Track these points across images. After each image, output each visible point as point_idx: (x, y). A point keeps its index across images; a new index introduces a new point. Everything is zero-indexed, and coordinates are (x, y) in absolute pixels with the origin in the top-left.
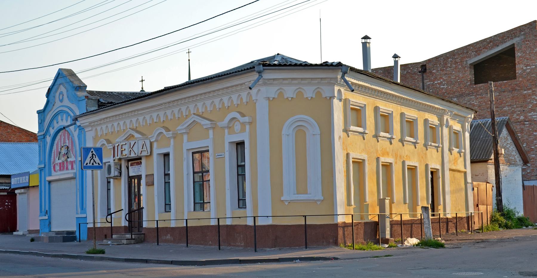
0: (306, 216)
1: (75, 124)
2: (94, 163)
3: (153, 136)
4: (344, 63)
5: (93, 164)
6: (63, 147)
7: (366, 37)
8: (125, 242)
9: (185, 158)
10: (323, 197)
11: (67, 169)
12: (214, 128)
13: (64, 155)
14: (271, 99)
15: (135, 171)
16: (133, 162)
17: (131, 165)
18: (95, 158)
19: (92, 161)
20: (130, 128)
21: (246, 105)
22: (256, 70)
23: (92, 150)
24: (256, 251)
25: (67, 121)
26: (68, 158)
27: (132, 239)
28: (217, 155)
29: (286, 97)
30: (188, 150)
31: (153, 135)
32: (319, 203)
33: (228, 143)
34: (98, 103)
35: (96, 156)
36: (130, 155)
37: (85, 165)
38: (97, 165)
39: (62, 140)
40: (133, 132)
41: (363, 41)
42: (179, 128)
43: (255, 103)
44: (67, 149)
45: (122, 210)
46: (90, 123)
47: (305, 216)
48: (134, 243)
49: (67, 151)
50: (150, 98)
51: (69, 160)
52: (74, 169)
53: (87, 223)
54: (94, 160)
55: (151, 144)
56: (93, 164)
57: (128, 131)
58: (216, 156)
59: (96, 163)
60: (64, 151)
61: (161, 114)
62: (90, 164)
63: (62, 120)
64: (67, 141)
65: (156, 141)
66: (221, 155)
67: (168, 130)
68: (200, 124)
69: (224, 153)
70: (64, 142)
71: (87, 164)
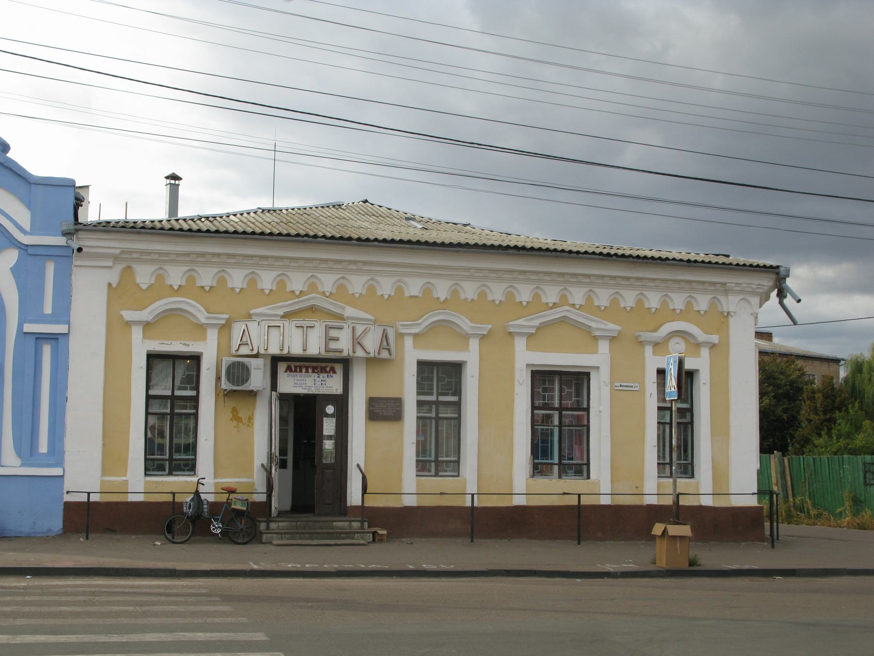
3: (419, 324)
7: (174, 177)
28: (618, 384)
41: (168, 181)
42: (520, 322)
50: (457, 252)
66: (631, 387)
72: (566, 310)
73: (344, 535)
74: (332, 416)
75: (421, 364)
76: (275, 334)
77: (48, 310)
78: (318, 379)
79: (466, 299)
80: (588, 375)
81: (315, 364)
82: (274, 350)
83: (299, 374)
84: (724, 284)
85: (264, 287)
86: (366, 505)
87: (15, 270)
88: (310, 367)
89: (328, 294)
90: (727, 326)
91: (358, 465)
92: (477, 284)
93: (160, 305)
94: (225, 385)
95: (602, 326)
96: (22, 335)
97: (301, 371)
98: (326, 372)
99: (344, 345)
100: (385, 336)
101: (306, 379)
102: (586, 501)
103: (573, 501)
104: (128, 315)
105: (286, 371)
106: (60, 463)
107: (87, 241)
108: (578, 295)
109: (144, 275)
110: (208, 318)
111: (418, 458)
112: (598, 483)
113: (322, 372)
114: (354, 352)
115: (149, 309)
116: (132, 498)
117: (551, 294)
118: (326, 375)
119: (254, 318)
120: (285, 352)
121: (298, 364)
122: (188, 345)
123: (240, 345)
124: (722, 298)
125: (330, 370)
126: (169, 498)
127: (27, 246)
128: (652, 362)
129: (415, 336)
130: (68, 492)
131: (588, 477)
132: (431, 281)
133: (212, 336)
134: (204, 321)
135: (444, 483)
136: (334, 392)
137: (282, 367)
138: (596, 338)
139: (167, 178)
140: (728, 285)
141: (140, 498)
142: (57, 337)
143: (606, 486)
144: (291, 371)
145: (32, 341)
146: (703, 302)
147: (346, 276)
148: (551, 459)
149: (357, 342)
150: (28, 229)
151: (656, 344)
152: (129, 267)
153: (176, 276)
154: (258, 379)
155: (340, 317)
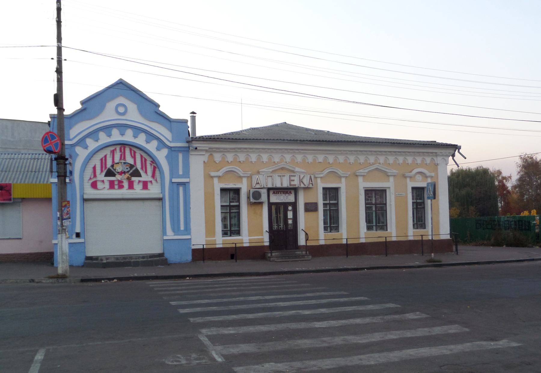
3: (323, 173)
28: (397, 194)
41: (191, 115)
42: (361, 171)
50: (338, 144)
66: (402, 194)
72: (378, 166)
74: (290, 210)
75: (324, 189)
76: (270, 179)
77: (181, 173)
78: (285, 196)
79: (340, 163)
80: (385, 190)
81: (284, 191)
82: (270, 186)
83: (278, 194)
84: (436, 153)
85: (252, 161)
86: (307, 245)
87: (167, 157)
88: (282, 192)
89: (288, 162)
90: (437, 169)
91: (302, 230)
92: (344, 156)
93: (224, 169)
94: (252, 200)
95: (391, 171)
96: (172, 183)
97: (278, 193)
98: (288, 193)
99: (296, 183)
100: (311, 178)
101: (280, 196)
102: (388, 240)
103: (383, 240)
104: (213, 174)
105: (273, 194)
106: (189, 234)
107: (195, 144)
108: (382, 159)
109: (218, 157)
110: (244, 174)
111: (324, 226)
112: (391, 233)
113: (286, 194)
114: (300, 185)
115: (221, 171)
116: (218, 246)
117: (372, 159)
118: (288, 195)
119: (261, 173)
120: (274, 186)
121: (277, 190)
122: (236, 185)
123: (256, 184)
124: (435, 158)
125: (289, 193)
126: (234, 246)
127: (171, 147)
128: (411, 184)
129: (321, 177)
130: (193, 245)
131: (387, 230)
132: (327, 156)
133: (245, 180)
134: (242, 175)
135: (333, 234)
136: (291, 201)
137: (271, 192)
138: (388, 176)
139: (191, 113)
140: (438, 153)
141: (221, 246)
142: (185, 183)
143: (394, 234)
144: (275, 194)
145: (175, 185)
146: (428, 160)
147: (295, 155)
148: (372, 224)
149: (301, 181)
150: (171, 140)
151: (411, 177)
152: (211, 154)
153: (230, 157)
154: (264, 198)
155: (293, 172)
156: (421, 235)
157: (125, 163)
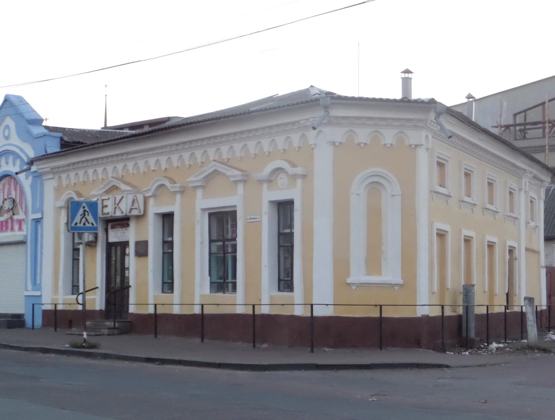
0: (382, 306)
1: (30, 169)
2: (87, 223)
3: (150, 190)
4: (438, 100)
5: (84, 224)
6: (6, 200)
7: (407, 71)
8: (106, 331)
9: (198, 221)
10: (402, 281)
11: (12, 229)
12: (244, 181)
13: (8, 210)
14: (337, 144)
15: (118, 236)
16: (115, 223)
17: (113, 227)
18: (88, 215)
19: (84, 220)
20: (112, 177)
21: (298, 151)
22: (321, 104)
23: (84, 205)
24: (312, 351)
25: (14, 165)
26: (14, 214)
27: (115, 328)
28: (248, 218)
29: (356, 142)
30: (204, 210)
31: (149, 188)
32: (396, 288)
33: (267, 202)
34: (61, 142)
35: (90, 214)
36: (115, 213)
37: (73, 225)
38: (90, 225)
39: (6, 190)
40: (119, 182)
41: (403, 75)
42: (192, 179)
43: (313, 149)
44: (12, 203)
45: (97, 288)
46: (52, 169)
47: (381, 306)
48: (118, 334)
49: (13, 205)
51: (15, 217)
52: (23, 231)
53: (43, 304)
54: (86, 219)
55: (146, 200)
56: (84, 224)
57: (111, 181)
58: (248, 219)
59: (89, 223)
60: (8, 205)
61: (163, 160)
62: (80, 223)
63: (7, 163)
64: (13, 192)
65: (154, 196)
66: (256, 218)
67: (173, 181)
68: (224, 174)
69: (261, 215)
70: (9, 193)
71: (76, 224)
73: (97, 330)
139: (402, 72)
142: (40, 220)
156: (201, 304)
157: (11, 198)
